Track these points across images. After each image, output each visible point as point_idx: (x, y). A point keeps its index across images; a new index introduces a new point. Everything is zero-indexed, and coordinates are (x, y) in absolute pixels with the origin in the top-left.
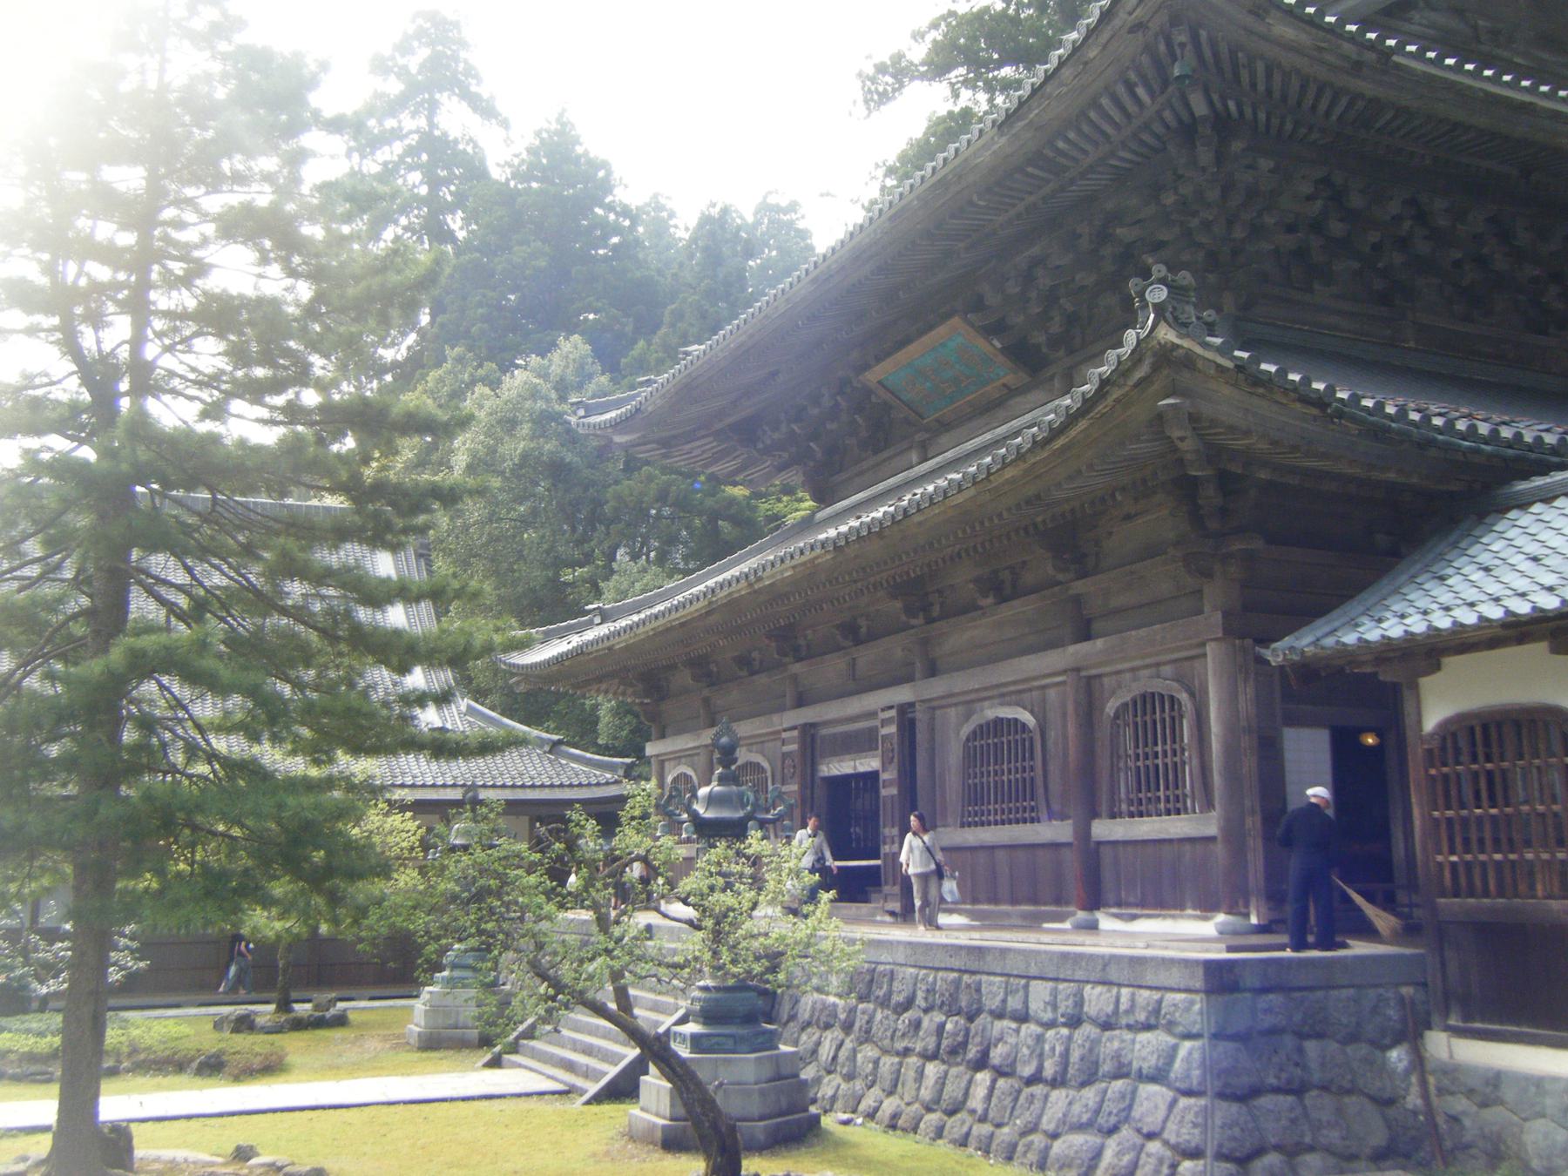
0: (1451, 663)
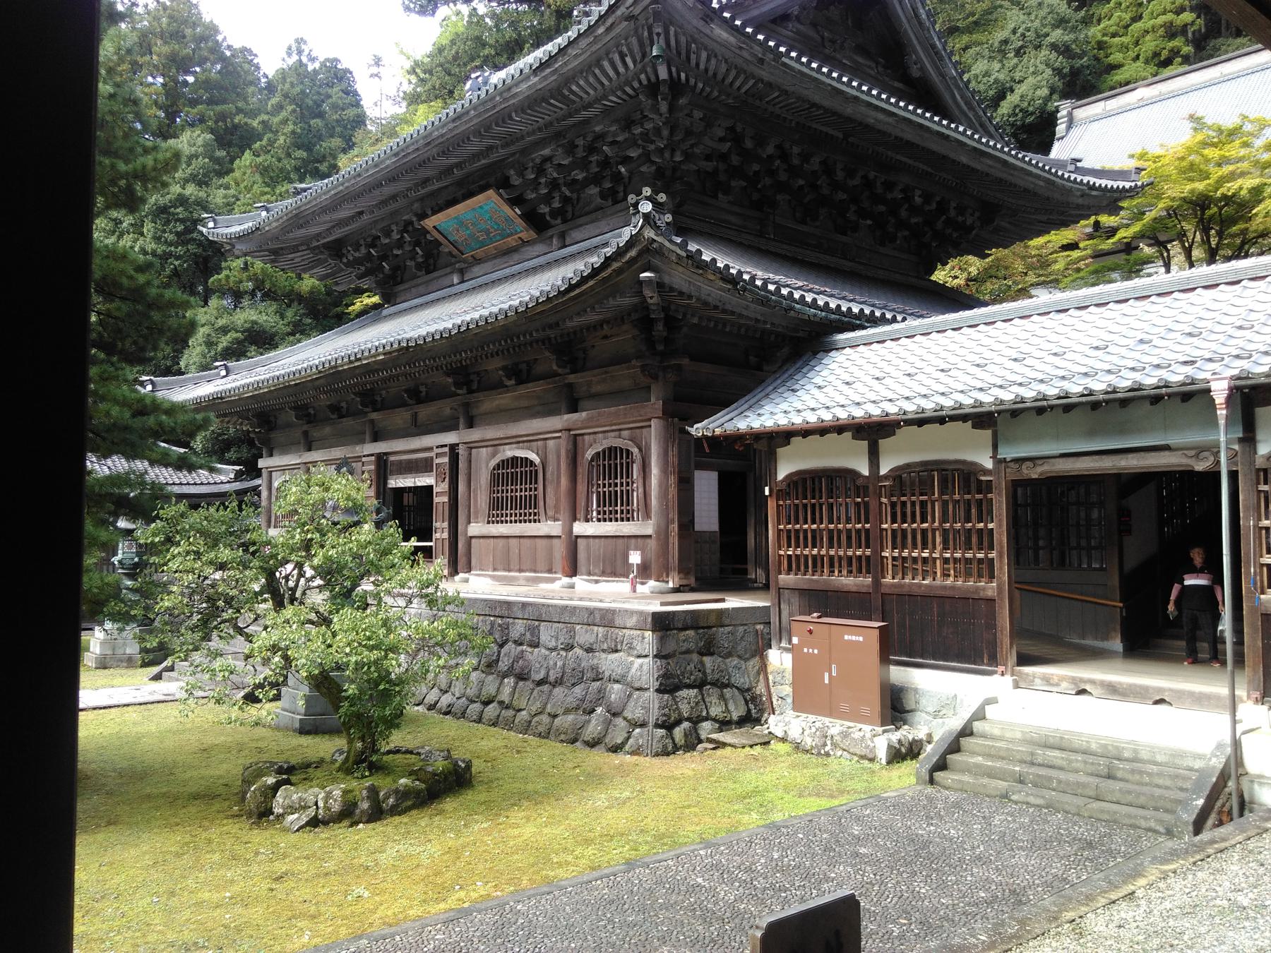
0: (796, 441)
